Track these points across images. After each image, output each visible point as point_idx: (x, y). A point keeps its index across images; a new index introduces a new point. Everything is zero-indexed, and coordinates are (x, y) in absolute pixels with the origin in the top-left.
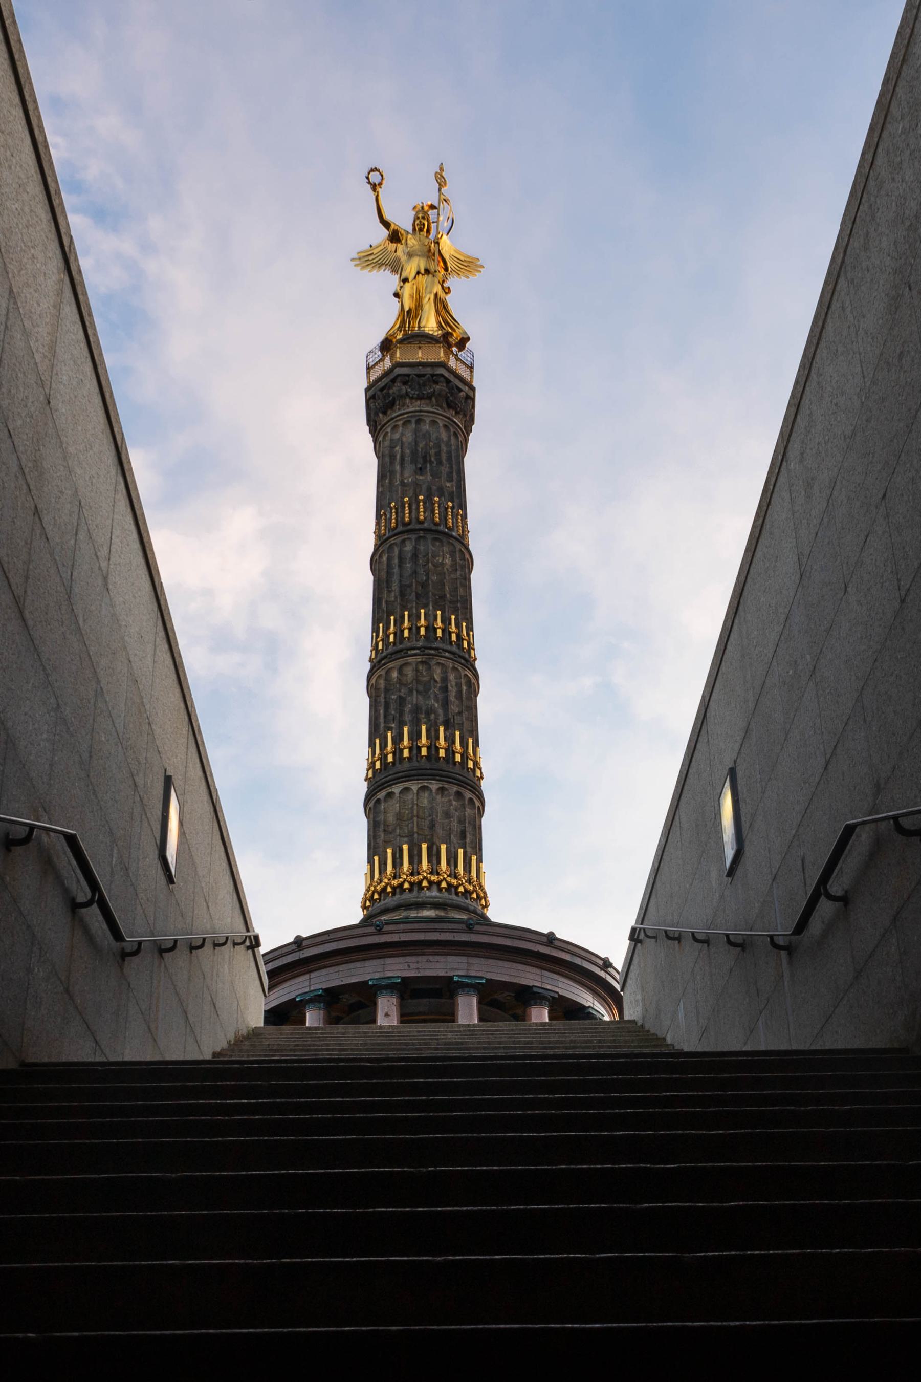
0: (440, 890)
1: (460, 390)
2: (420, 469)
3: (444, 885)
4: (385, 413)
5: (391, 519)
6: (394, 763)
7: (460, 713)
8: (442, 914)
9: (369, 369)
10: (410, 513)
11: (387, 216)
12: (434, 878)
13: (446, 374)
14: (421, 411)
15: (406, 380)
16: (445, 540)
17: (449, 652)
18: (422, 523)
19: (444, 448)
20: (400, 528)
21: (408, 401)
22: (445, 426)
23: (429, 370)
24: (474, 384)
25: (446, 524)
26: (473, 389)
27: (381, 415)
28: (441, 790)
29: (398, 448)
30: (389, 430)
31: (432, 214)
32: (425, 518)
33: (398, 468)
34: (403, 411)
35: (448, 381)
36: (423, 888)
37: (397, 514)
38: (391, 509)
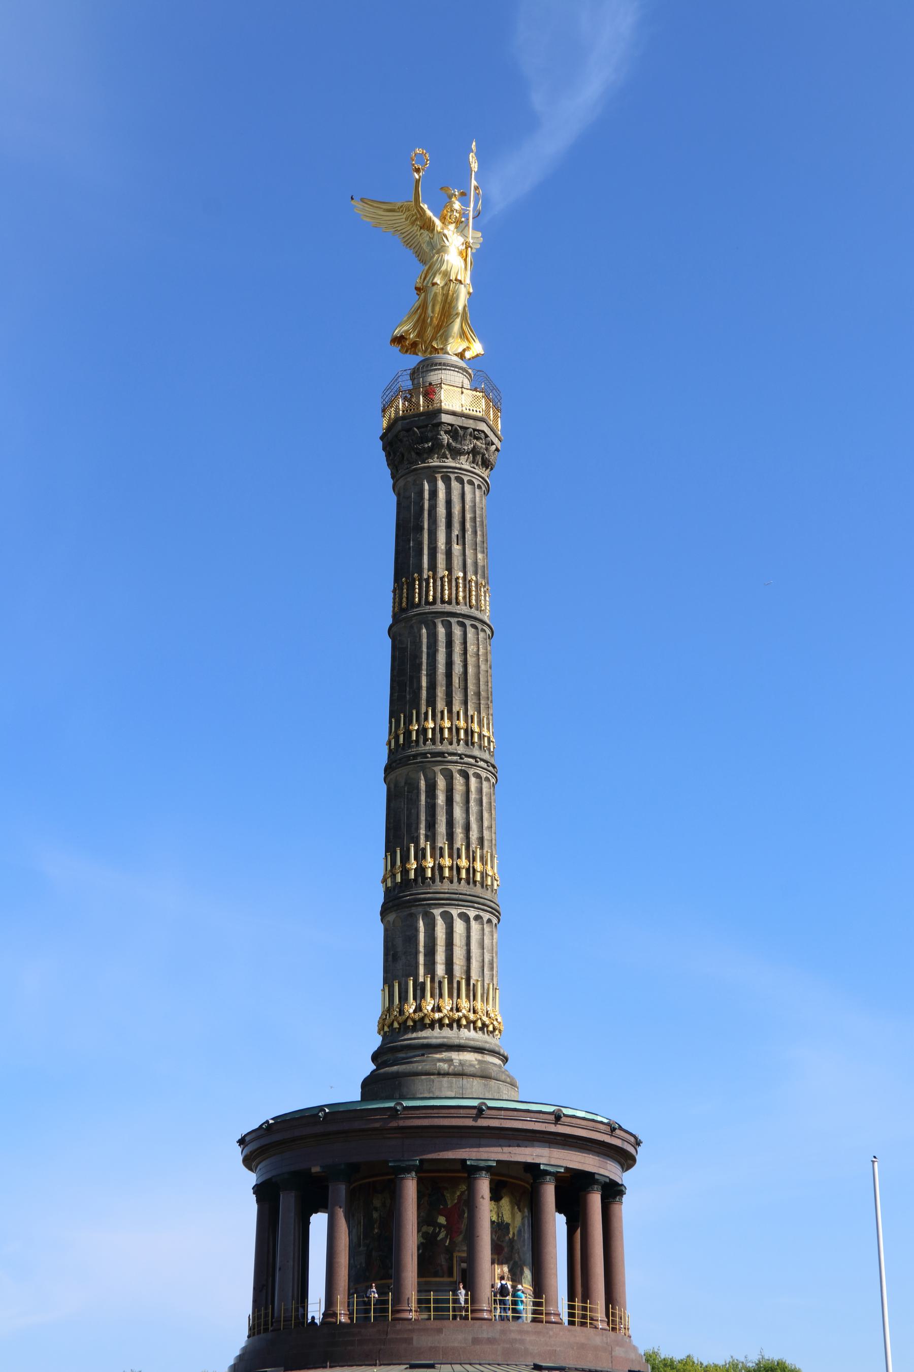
0: (475, 1029)
1: (493, 444)
3: (479, 1024)
6: (433, 879)
7: (490, 827)
8: (479, 1056)
10: (450, 589)
12: (472, 1016)
14: (460, 469)
16: (479, 626)
17: (486, 762)
19: (478, 512)
27: (413, 453)
28: (478, 918)
35: (486, 436)
36: (459, 1026)
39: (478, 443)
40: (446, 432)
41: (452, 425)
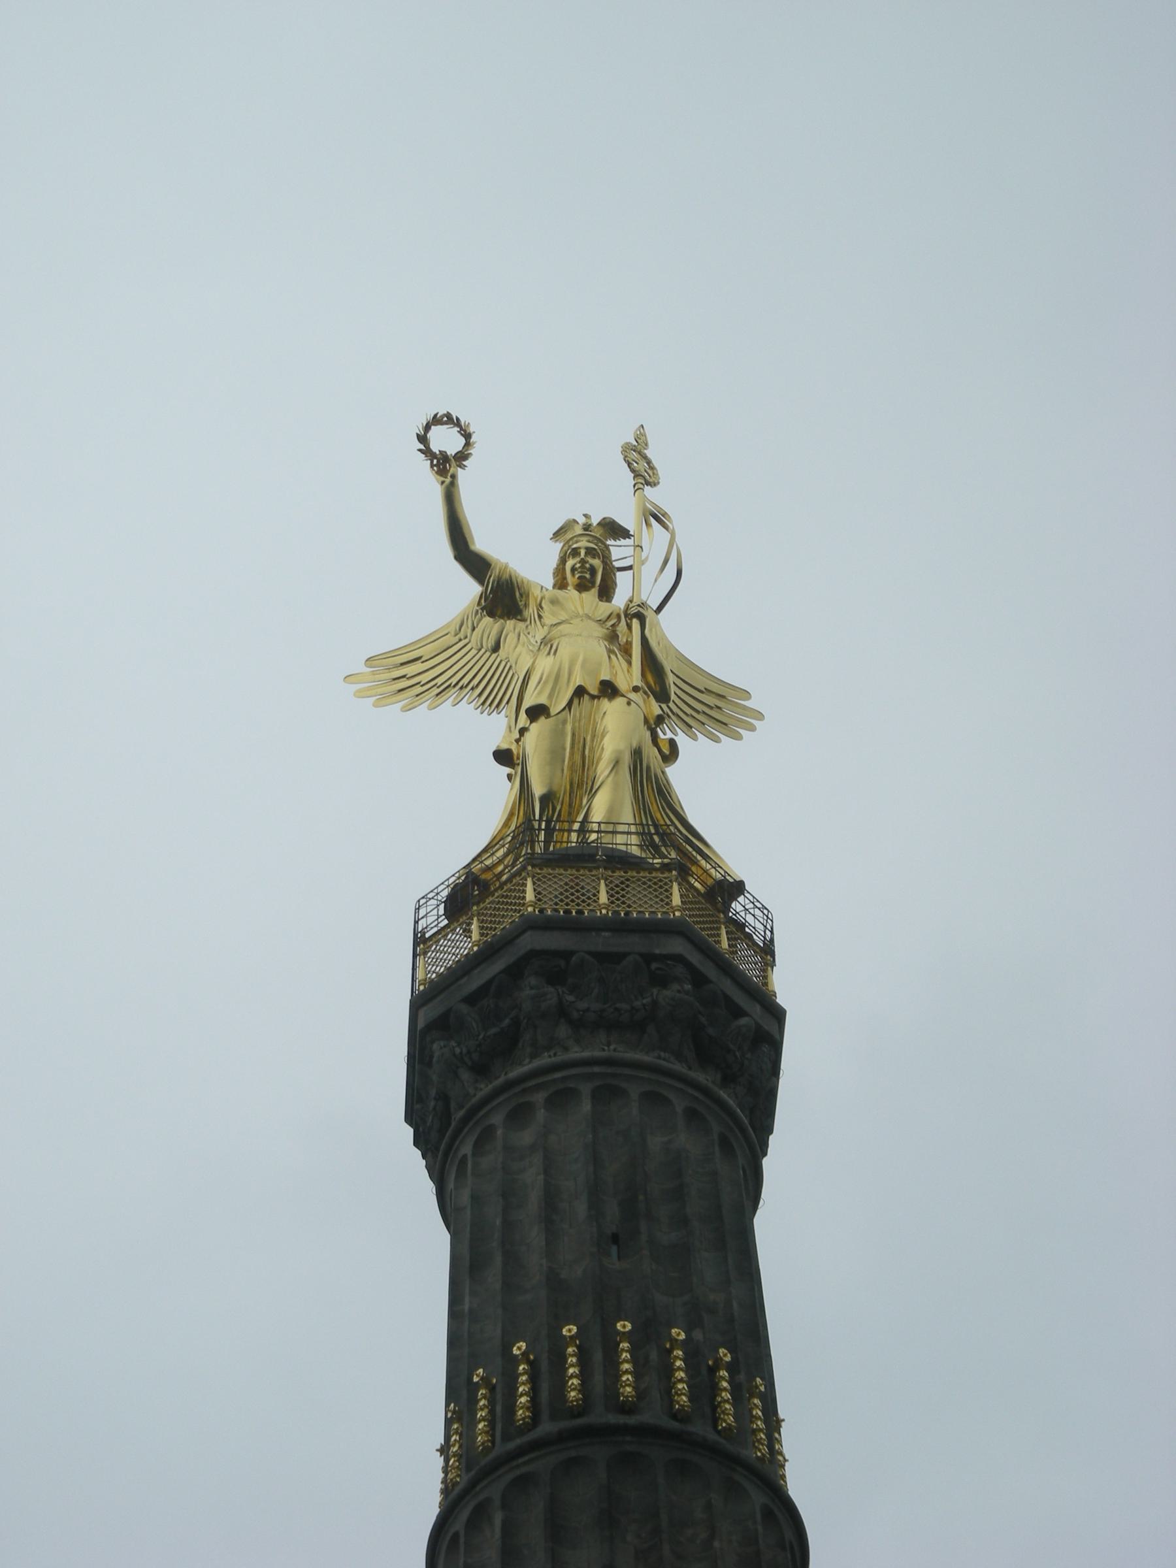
1: (738, 1012)
2: (615, 1239)
4: (481, 1070)
5: (512, 1394)
9: (421, 942)
10: (584, 1375)
11: (481, 543)
13: (695, 958)
15: (556, 968)
18: (626, 1409)
20: (547, 1427)
21: (563, 1031)
22: (692, 1115)
23: (634, 944)
24: (781, 1000)
25: (715, 1421)
26: (778, 1015)
27: (465, 1075)
29: (532, 1176)
30: (497, 1119)
31: (619, 551)
32: (641, 1394)
33: (535, 1236)
34: (545, 1060)
37: (534, 1379)
38: (515, 1361)
39: (667, 993)
40: (555, 978)
41: (566, 955)
